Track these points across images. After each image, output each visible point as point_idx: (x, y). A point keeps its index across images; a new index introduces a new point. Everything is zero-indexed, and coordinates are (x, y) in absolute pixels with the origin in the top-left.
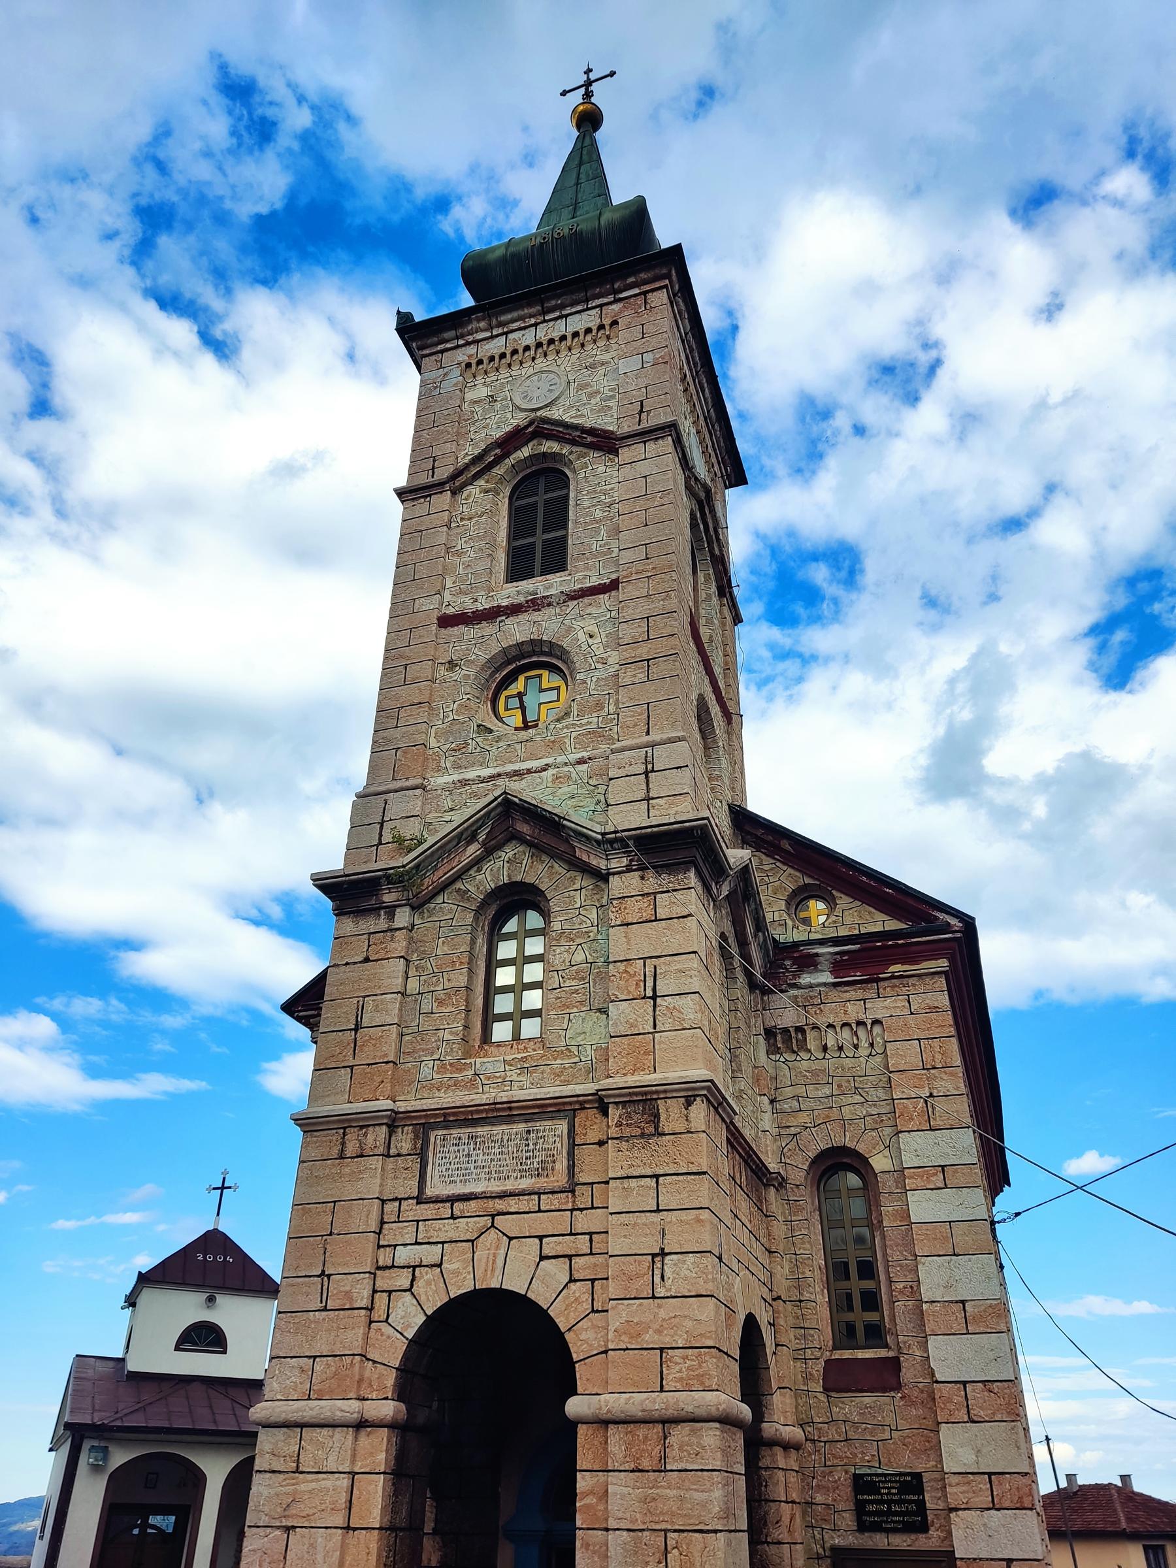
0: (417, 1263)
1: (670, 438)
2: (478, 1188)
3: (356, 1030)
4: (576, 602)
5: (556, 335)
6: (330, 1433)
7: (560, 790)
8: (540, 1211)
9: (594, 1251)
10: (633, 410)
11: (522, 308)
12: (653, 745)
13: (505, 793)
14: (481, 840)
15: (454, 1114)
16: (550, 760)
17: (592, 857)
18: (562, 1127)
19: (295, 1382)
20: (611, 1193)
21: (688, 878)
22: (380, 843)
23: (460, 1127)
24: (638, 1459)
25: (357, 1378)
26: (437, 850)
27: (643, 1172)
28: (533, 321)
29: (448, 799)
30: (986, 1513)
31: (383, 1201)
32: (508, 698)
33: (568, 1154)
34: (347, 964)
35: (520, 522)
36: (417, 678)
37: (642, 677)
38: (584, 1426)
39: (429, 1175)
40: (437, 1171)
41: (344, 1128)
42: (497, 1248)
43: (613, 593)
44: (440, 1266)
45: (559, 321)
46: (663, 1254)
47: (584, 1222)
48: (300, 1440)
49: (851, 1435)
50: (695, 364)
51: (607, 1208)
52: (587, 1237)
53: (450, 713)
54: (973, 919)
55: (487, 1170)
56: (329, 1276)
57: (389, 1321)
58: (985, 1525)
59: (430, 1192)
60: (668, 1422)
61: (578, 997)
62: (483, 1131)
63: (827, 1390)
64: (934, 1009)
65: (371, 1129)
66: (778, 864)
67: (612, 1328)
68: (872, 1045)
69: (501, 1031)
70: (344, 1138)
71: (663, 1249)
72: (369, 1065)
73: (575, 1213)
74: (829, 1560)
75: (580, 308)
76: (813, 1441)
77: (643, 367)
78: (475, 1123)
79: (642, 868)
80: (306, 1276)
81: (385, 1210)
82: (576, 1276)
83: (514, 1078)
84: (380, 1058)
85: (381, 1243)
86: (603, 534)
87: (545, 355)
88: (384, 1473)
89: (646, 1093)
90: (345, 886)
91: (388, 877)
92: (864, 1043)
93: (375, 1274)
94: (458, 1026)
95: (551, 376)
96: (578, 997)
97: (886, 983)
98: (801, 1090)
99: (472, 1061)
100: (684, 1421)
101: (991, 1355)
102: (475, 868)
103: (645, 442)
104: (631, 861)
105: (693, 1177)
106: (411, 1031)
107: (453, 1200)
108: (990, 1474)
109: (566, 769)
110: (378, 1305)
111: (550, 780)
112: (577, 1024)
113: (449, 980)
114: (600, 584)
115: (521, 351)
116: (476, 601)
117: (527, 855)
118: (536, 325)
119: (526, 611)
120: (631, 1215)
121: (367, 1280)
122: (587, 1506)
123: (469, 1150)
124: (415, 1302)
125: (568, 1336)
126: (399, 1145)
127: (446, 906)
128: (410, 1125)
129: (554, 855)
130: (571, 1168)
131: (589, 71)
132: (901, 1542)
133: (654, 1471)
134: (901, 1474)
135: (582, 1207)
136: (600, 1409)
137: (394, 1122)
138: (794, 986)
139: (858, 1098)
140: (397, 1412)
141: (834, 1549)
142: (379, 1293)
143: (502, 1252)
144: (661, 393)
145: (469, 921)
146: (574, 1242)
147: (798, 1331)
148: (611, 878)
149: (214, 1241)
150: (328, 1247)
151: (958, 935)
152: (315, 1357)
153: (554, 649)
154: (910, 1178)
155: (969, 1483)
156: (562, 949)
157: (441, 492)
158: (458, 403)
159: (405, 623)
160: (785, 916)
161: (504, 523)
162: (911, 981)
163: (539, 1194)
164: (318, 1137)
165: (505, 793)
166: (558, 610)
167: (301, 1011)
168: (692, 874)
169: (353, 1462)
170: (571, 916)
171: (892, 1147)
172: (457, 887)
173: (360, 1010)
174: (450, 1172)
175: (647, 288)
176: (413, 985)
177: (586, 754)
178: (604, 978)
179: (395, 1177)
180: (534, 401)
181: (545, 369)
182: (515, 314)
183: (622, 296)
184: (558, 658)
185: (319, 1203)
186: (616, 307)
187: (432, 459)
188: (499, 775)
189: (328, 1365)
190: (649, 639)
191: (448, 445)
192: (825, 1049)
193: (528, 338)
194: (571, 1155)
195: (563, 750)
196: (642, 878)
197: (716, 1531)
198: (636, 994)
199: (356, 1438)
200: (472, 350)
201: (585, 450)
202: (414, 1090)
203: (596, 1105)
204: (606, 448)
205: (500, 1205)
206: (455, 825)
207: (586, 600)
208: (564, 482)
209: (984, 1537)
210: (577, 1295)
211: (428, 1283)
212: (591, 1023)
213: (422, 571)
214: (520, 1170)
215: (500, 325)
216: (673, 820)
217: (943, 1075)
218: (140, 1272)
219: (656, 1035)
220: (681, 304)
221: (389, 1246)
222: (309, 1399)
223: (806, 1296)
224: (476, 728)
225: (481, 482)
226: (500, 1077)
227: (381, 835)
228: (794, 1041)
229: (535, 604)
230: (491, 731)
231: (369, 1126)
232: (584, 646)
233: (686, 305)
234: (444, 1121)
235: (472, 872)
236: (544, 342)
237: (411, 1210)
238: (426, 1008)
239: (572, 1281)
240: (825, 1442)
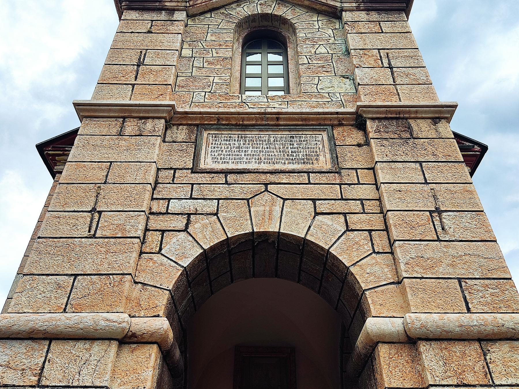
0: (192, 212)
6: (87, 346)
8: (309, 183)
15: (227, 119)
24: (460, 374)
33: (330, 150)
38: (386, 346)
40: (209, 155)
41: (124, 118)
44: (216, 214)
48: (47, 352)
55: (257, 157)
56: (100, 212)
57: (163, 252)
59: (202, 166)
62: (251, 134)
65: (150, 120)
70: (123, 123)
72: (149, 85)
73: (343, 186)
78: (244, 127)
79: (367, 10)
80: (74, 211)
85: (155, 196)
100: (500, 340)
102: (236, 4)
106: (186, 75)
107: (226, 172)
110: (150, 240)
117: (275, 3)
120: (402, 185)
121: (143, 217)
124: (190, 238)
125: (352, 269)
128: (184, 125)
130: (335, 159)
135: (348, 183)
142: (151, 232)
143: (278, 209)
146: (346, 205)
148: (344, 13)
152: (76, 276)
164: (98, 121)
170: (312, 31)
172: (222, 12)
173: (143, 56)
174: (222, 156)
176: (186, 52)
185: (95, 162)
196: (367, 14)
214: (287, 159)
221: (163, 199)
231: (148, 118)
235: (233, 6)
239: (348, 230)
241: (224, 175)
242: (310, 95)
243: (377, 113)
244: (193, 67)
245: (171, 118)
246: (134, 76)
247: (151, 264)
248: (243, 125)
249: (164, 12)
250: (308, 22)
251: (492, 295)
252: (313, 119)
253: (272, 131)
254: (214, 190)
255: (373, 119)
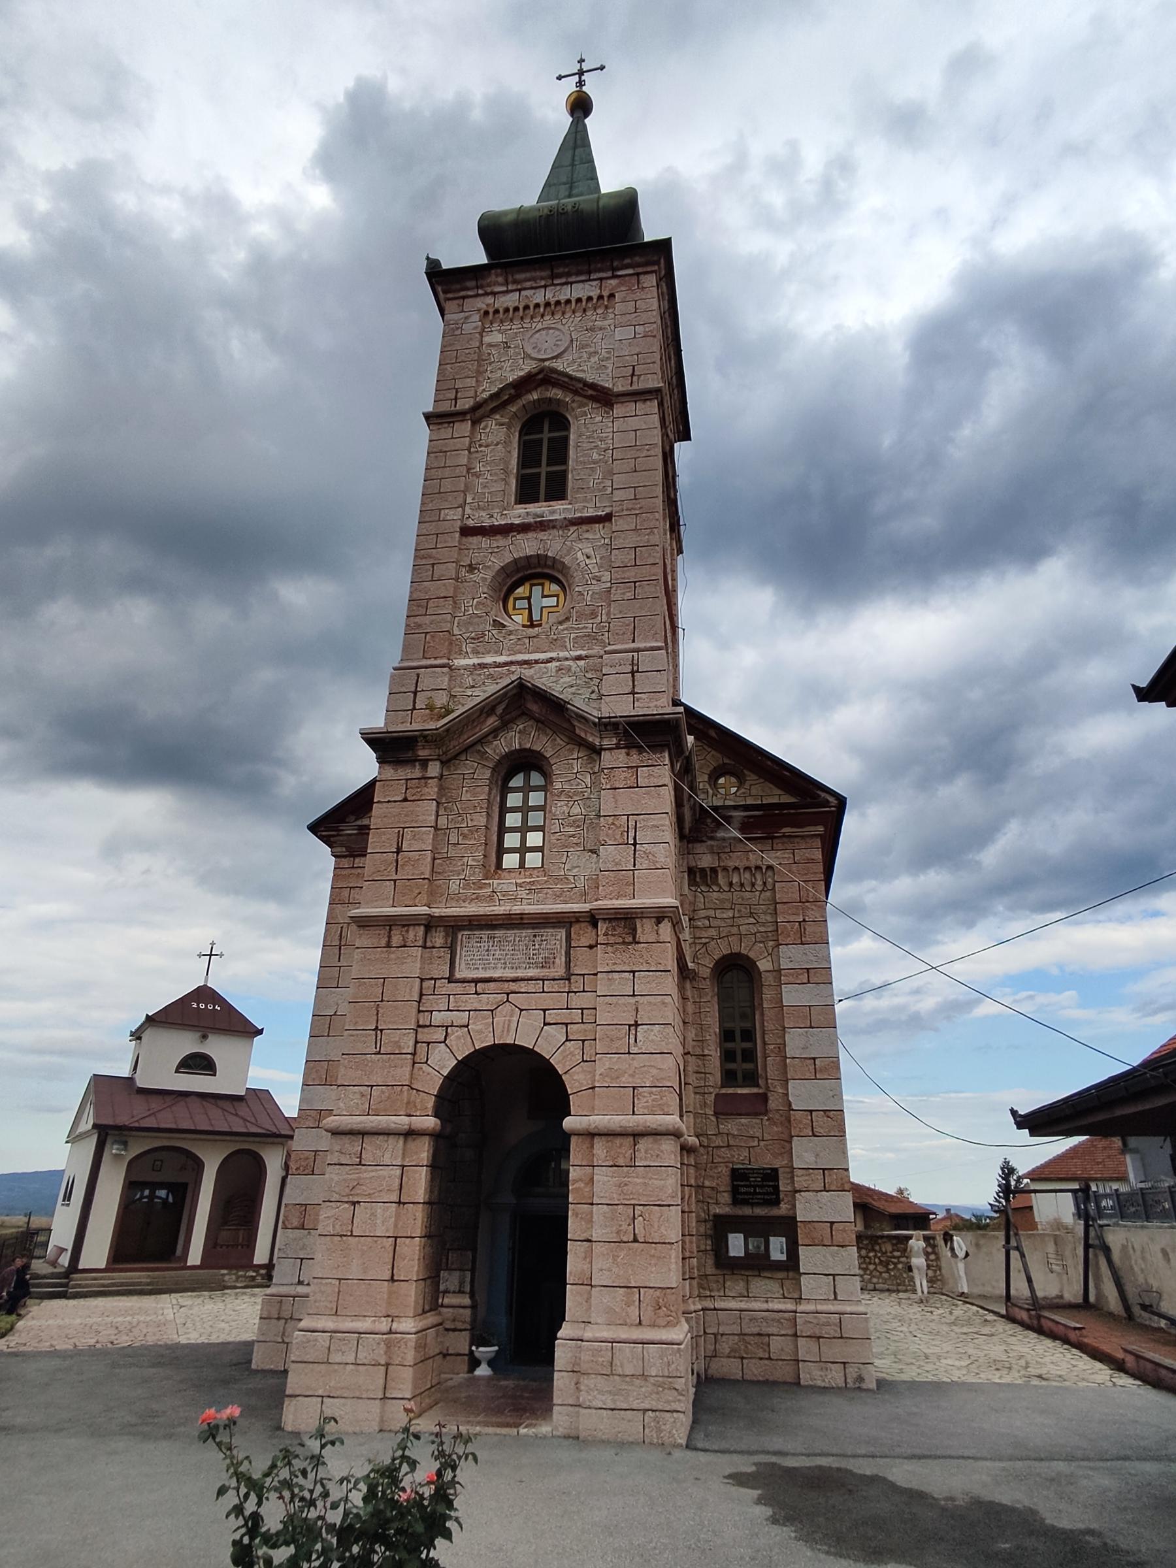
1: (656, 401)
2: (496, 974)
3: (398, 853)
4: (576, 528)
5: (563, 298)
7: (562, 680)
8: (543, 992)
9: (584, 1021)
10: (627, 373)
11: (535, 270)
12: (638, 650)
13: (520, 678)
14: (498, 714)
15: (478, 920)
16: (554, 655)
17: (588, 735)
18: (562, 934)
19: (358, 1104)
20: (599, 982)
21: (664, 757)
22: (414, 708)
23: (482, 929)
25: (405, 1101)
26: (464, 718)
27: (623, 969)
28: (543, 283)
29: (470, 678)
30: (819, 1193)
31: (422, 980)
32: (516, 599)
33: (566, 953)
34: (389, 802)
35: (528, 456)
36: (443, 576)
37: (630, 595)
38: (576, 1137)
39: (457, 962)
41: (390, 926)
42: (512, 1016)
43: (607, 524)
45: (565, 287)
46: (636, 1025)
47: (577, 1001)
49: (731, 1143)
50: (667, 338)
51: (596, 992)
52: (580, 1011)
53: (470, 608)
54: (846, 798)
56: (381, 1030)
57: (428, 1062)
58: (818, 1201)
59: (458, 975)
60: (637, 1135)
61: (575, 840)
62: (499, 933)
63: (716, 1114)
64: (812, 861)
65: (411, 928)
66: (705, 746)
67: (598, 1072)
68: (765, 883)
69: (511, 860)
70: (390, 932)
71: (636, 1022)
73: (570, 994)
74: (711, 1223)
75: (583, 278)
76: (704, 1146)
77: (635, 337)
81: (424, 986)
82: (569, 1038)
83: (524, 896)
84: (418, 875)
85: (421, 1009)
86: (599, 474)
87: (553, 314)
88: (426, 1166)
89: (627, 913)
90: (387, 740)
91: (425, 737)
92: (759, 882)
93: (416, 1030)
94: (479, 855)
95: (557, 333)
96: (575, 840)
97: (777, 841)
98: (711, 913)
99: (491, 881)
101: (831, 1093)
102: (493, 735)
103: (636, 402)
104: (620, 740)
105: (660, 973)
107: (476, 981)
108: (824, 1170)
109: (567, 663)
111: (554, 670)
112: (573, 858)
113: (472, 820)
114: (597, 515)
115: (532, 307)
116: (492, 516)
118: (545, 287)
119: (534, 530)
122: (576, 1189)
123: (489, 946)
126: (433, 940)
127: (468, 766)
129: (556, 730)
131: (581, 61)
132: (760, 1211)
133: (627, 1166)
134: (764, 1169)
136: (590, 1125)
137: (430, 924)
138: (712, 838)
139: (752, 920)
140: (436, 1124)
141: (716, 1216)
143: (515, 1019)
144: (649, 361)
145: (488, 776)
147: (698, 1075)
148: (603, 753)
149: (204, 993)
150: (379, 1009)
151: (833, 809)
152: (372, 1086)
153: (555, 563)
154: (785, 976)
155: (809, 1175)
156: (563, 803)
157: (462, 421)
158: (477, 344)
159: (431, 528)
160: (707, 786)
161: (515, 454)
162: (797, 840)
163: (543, 980)
165: (520, 678)
166: (561, 532)
167: (323, 831)
168: (667, 755)
169: (403, 1158)
171: (773, 954)
174: (474, 961)
175: (640, 270)
177: (583, 653)
178: (594, 827)
179: (431, 963)
180: (542, 352)
181: (553, 326)
182: (528, 275)
183: (620, 273)
184: (559, 571)
186: (614, 282)
187: (454, 391)
188: (512, 663)
189: (383, 1092)
190: (636, 565)
191: (469, 380)
192: (731, 884)
193: (539, 297)
194: (568, 954)
195: (564, 647)
196: (628, 754)
197: (669, 1206)
198: (621, 842)
199: (405, 1142)
200: (490, 300)
201: (585, 400)
202: (445, 900)
203: (588, 920)
204: (603, 402)
205: (513, 986)
206: (479, 700)
207: (584, 527)
208: (564, 425)
209: (818, 1208)
210: (572, 1049)
211: (458, 1038)
212: (584, 860)
213: (447, 485)
215: (515, 282)
216: (655, 712)
217: (813, 907)
218: (147, 1015)
219: (636, 872)
220: (665, 287)
222: (368, 1115)
223: (706, 1052)
224: (491, 622)
225: (498, 417)
226: (513, 895)
227: (414, 702)
228: (709, 878)
229: (542, 526)
230: (504, 626)
231: (409, 925)
232: (583, 565)
233: (668, 288)
234: (469, 925)
235: (490, 738)
236: (552, 303)
237: (444, 987)
238: (453, 840)
239: (567, 1040)
240: (713, 1148)
241: (473, 984)
242: (558, 879)
243: (607, 914)
244: (448, 844)
245: (430, 922)
246: (394, 868)
247: (421, 1073)
248: (492, 925)
249: (417, 764)
250: (566, 762)
251: (653, 1100)
252: (553, 918)
253: (519, 929)
254: (466, 1001)
255: (604, 919)
